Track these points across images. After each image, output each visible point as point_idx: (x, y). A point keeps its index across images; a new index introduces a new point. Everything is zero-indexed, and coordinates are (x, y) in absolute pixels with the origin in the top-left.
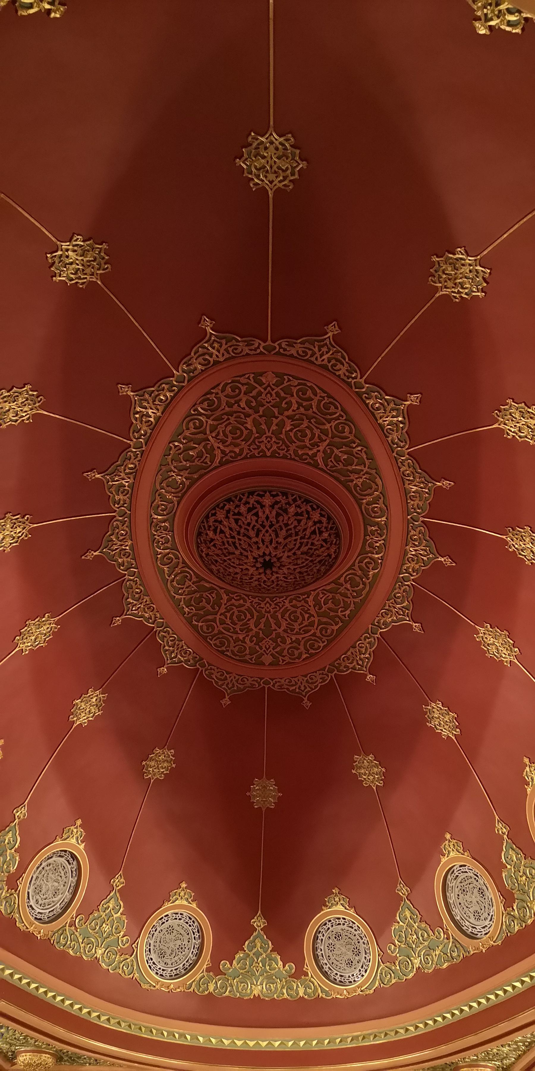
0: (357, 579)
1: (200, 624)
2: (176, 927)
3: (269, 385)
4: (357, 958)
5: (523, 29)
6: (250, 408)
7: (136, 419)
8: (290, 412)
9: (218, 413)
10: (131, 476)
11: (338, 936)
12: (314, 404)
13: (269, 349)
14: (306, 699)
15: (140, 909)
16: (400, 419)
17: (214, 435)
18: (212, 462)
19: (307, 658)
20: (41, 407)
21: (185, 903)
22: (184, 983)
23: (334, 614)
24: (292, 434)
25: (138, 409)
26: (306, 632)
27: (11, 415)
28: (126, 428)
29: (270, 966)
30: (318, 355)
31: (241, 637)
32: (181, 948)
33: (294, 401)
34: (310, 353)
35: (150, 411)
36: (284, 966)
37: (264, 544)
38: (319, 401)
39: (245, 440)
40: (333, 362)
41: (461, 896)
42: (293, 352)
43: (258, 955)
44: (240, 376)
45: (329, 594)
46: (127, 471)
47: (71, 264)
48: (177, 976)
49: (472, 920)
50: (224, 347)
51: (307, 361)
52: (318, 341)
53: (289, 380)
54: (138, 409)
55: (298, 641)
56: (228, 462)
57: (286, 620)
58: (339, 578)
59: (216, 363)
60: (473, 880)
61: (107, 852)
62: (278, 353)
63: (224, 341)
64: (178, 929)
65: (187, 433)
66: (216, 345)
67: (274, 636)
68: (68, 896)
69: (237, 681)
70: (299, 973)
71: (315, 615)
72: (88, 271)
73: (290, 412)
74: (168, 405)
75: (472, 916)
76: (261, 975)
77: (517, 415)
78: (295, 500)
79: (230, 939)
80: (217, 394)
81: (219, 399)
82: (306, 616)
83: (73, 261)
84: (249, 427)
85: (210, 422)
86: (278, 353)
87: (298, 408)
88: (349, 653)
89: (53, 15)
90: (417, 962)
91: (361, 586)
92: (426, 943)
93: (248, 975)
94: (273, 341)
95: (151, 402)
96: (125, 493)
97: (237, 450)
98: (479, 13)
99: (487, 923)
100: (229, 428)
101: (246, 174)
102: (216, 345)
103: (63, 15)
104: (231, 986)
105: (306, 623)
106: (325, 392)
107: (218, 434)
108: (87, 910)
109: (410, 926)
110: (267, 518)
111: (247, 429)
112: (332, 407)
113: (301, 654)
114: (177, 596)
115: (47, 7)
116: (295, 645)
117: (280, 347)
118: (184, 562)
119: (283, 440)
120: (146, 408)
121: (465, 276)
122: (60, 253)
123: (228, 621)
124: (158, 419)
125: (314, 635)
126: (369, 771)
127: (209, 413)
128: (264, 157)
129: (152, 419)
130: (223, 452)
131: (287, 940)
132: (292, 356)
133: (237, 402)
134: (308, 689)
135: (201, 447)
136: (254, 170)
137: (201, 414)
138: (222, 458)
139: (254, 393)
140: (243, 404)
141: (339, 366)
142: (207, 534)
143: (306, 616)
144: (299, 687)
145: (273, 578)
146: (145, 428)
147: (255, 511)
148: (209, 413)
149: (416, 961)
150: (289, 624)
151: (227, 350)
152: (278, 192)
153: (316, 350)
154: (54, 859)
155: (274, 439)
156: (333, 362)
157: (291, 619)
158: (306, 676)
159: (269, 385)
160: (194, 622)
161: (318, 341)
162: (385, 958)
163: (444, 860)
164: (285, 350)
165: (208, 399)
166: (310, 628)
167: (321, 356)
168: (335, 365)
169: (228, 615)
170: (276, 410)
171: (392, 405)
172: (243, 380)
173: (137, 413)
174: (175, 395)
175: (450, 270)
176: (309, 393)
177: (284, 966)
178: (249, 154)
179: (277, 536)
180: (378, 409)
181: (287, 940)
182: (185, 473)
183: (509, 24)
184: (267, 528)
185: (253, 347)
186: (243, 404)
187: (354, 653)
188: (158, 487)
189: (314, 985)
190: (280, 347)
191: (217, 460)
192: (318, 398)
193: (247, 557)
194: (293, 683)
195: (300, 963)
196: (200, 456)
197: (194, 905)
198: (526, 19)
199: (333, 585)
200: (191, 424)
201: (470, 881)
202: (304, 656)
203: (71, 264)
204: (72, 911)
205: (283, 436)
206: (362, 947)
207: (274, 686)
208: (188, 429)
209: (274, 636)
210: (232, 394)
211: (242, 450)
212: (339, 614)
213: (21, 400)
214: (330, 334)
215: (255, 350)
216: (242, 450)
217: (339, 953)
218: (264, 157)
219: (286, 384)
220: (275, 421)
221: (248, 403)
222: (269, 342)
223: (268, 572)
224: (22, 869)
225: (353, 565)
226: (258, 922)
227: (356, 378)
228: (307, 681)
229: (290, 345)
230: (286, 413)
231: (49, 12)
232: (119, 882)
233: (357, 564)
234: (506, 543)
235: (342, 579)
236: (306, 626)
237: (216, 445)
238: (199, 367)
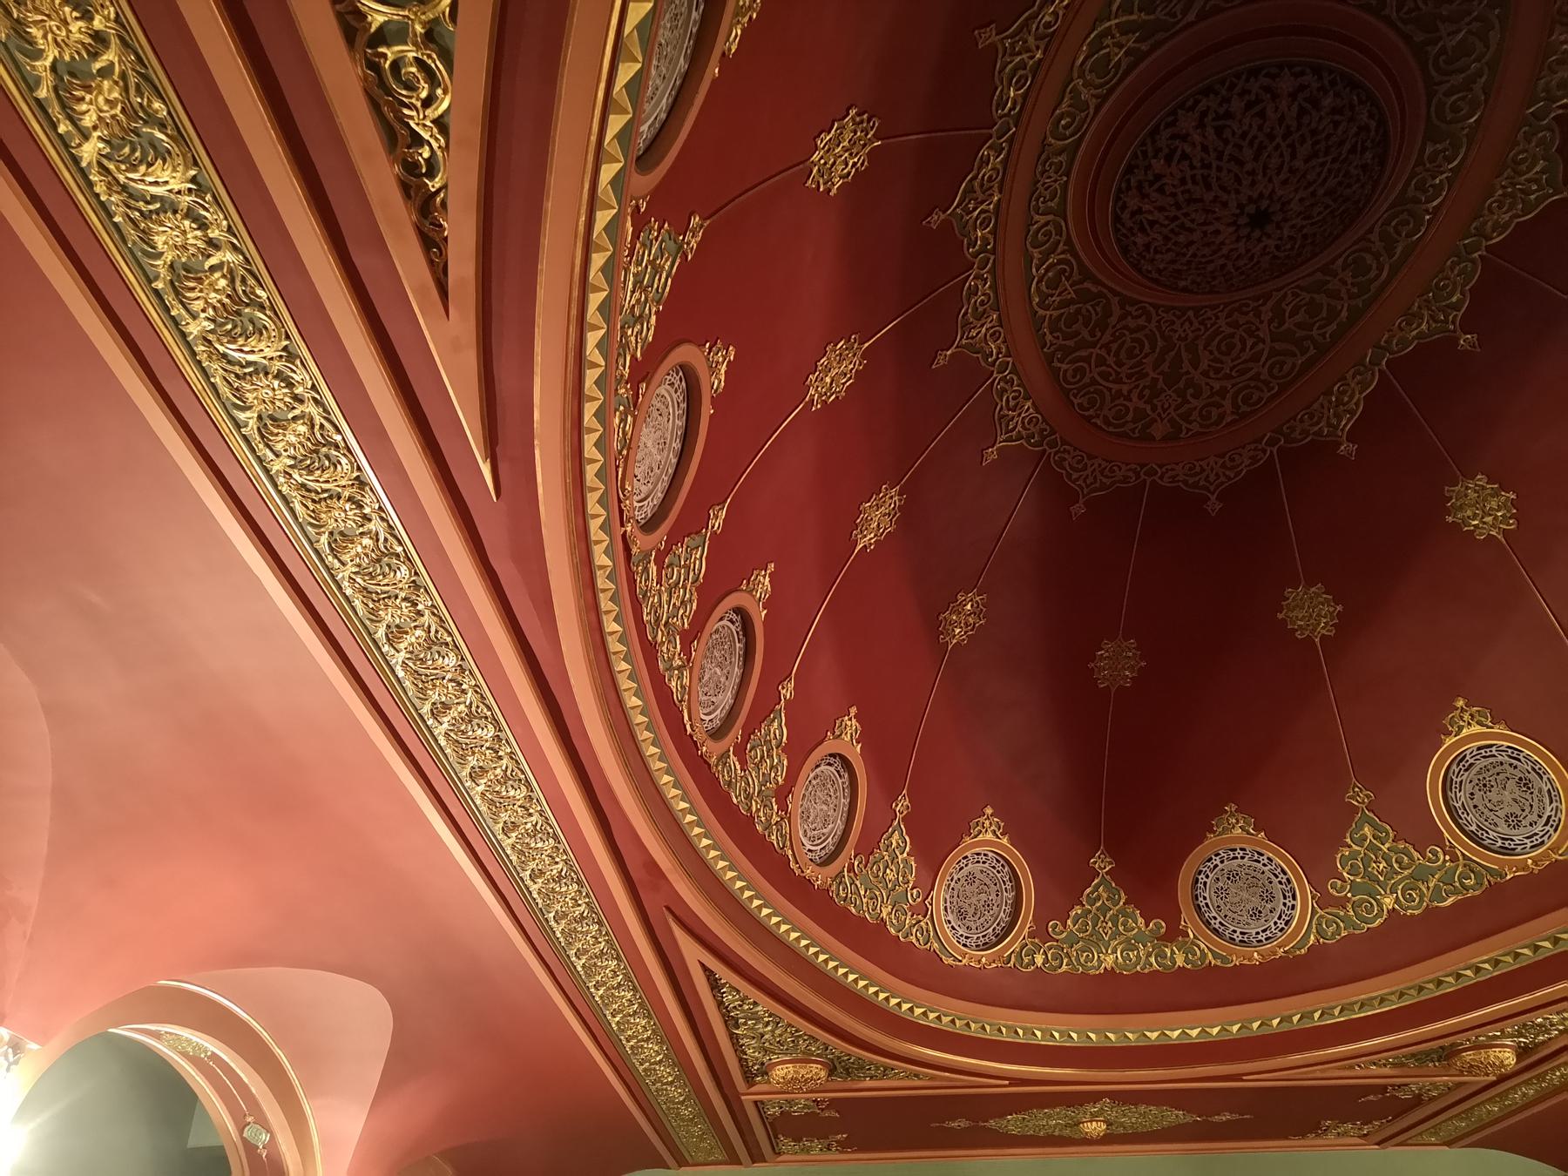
0: (1369, 258)
1: (1064, 366)
2: (978, 875)
4: (1269, 906)
11: (1232, 876)
14: (1213, 498)
15: (933, 849)
19: (1233, 422)
21: (989, 836)
22: (999, 955)
23: (1304, 333)
26: (1242, 373)
29: (1124, 924)
31: (1125, 389)
32: (987, 905)
36: (1147, 925)
37: (1229, 193)
41: (1478, 795)
43: (1104, 910)
45: (1304, 294)
48: (988, 946)
49: (1503, 828)
55: (1223, 393)
57: (1211, 352)
58: (1333, 261)
60: (1506, 766)
61: (887, 758)
64: (981, 876)
67: (1181, 385)
68: (840, 825)
69: (1102, 473)
70: (1174, 934)
71: (1268, 340)
75: (1501, 823)
76: (1113, 938)
78: (1333, 83)
79: (1063, 889)
82: (1249, 343)
88: (1316, 406)
90: (1388, 902)
91: (1373, 274)
92: (1406, 873)
93: (1095, 941)
99: (1538, 829)
104: (1068, 955)
105: (1245, 356)
108: (868, 847)
109: (1372, 848)
110: (1282, 119)
113: (1221, 417)
114: (1041, 312)
116: (1217, 398)
118: (1069, 242)
123: (1111, 360)
125: (1256, 377)
126: (1311, 613)
131: (1153, 886)
134: (1223, 479)
142: (1149, 167)
143: (1249, 343)
144: (1207, 479)
145: (1286, 232)
147: (1257, 109)
149: (1387, 900)
150: (1215, 360)
154: (822, 767)
157: (1221, 353)
158: (1222, 456)
160: (1056, 364)
162: (1324, 901)
163: (1449, 741)
166: (1250, 365)
169: (1114, 346)
177: (1147, 925)
179: (1293, 156)
181: (1153, 886)
184: (1279, 140)
187: (1326, 405)
189: (1199, 949)
193: (1225, 205)
194: (1198, 469)
195: (1172, 917)
197: (1005, 841)
199: (1319, 275)
201: (1498, 769)
202: (1229, 419)
204: (849, 850)
206: (1277, 889)
207: (1161, 478)
209: (1181, 385)
212: (1315, 332)
217: (1237, 899)
223: (1269, 228)
224: (792, 778)
225: (1371, 231)
226: (1102, 863)
228: (1223, 466)
232: (902, 805)
233: (1377, 229)
236: (1246, 361)
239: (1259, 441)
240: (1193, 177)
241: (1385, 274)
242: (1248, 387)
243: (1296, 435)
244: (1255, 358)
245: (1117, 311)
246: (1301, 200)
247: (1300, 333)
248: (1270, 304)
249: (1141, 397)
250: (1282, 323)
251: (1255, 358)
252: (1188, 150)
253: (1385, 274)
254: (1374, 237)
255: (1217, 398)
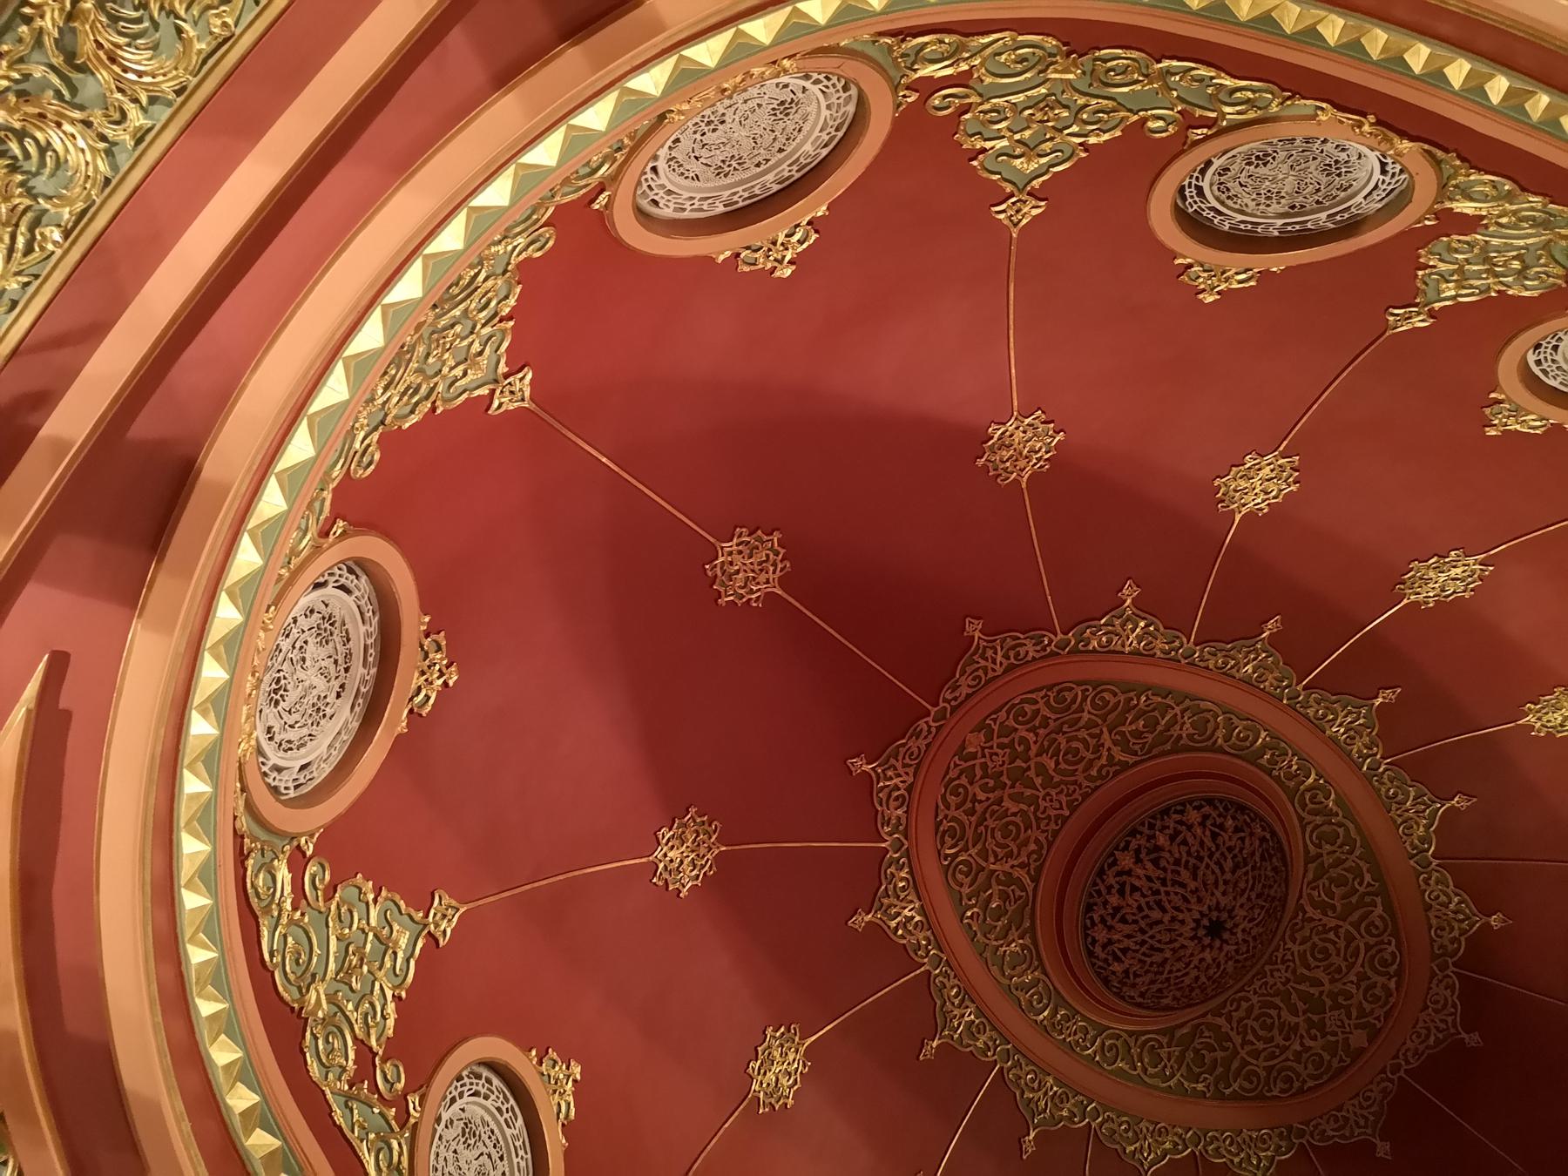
3: (983, 749)
5: (816, 232)
6: (993, 790)
7: (902, 937)
8: (1034, 749)
9: (970, 833)
10: (967, 1003)
12: (1046, 712)
13: (941, 716)
14: (1464, 1035)
16: (1142, 624)
17: (992, 860)
18: (1023, 889)
20: (803, 1038)
24: (1063, 766)
25: (893, 924)
27: (784, 1081)
28: (905, 958)
30: (990, 665)
33: (1024, 734)
34: (980, 673)
35: (906, 912)
38: (1047, 704)
39: (1028, 827)
40: (1012, 654)
42: (965, 691)
44: (947, 773)
46: (956, 1002)
47: (682, 862)
50: (899, 765)
51: (987, 682)
52: (974, 654)
53: (995, 720)
54: (893, 924)
55: (1362, 977)
56: (1039, 870)
58: (1307, 851)
59: (909, 790)
62: (954, 709)
63: (892, 761)
65: (966, 890)
66: (890, 773)
67: (1329, 1002)
69: (1362, 1107)
72: (702, 851)
73: (1034, 749)
74: (915, 884)
77: (1243, 484)
78: (1152, 827)
80: (946, 817)
81: (954, 819)
82: (1331, 935)
83: (681, 858)
84: (1014, 810)
85: (973, 851)
86: (954, 709)
87: (1037, 735)
88: (1434, 921)
89: (451, 683)
91: (1341, 831)
94: (936, 704)
95: (895, 902)
96: (981, 1029)
97: (1033, 847)
98: (769, 266)
100: (998, 834)
101: (739, 603)
102: (890, 773)
103: (459, 672)
105: (1342, 944)
106: (1040, 690)
107: (996, 856)
110: (1149, 879)
111: (1014, 814)
112: (1066, 694)
113: (1384, 986)
114: (1171, 1083)
115: (440, 682)
116: (1364, 985)
117: (949, 702)
118: (1131, 1034)
119: (1061, 782)
120: (899, 914)
121: (1026, 442)
122: (661, 866)
123: (1260, 1045)
124: (922, 911)
125: (1368, 948)
127: (961, 844)
128: (738, 572)
129: (918, 918)
130: (1022, 866)
132: (968, 696)
133: (974, 800)
135: (996, 888)
136: (742, 591)
137: (956, 855)
138: (1028, 873)
139: (979, 772)
140: (981, 796)
141: (1022, 651)
142: (1114, 973)
143: (1331, 935)
145: (1240, 935)
146: (921, 936)
147: (1128, 889)
148: (961, 844)
151: (904, 766)
152: (783, 582)
153: (983, 663)
155: (1053, 792)
156: (1012, 654)
157: (1320, 960)
159: (983, 749)
160: (1227, 1092)
161: (974, 654)
164: (955, 699)
165: (944, 832)
166: (1353, 945)
167: (994, 662)
168: (1018, 654)
169: (1250, 1037)
170: (1019, 763)
171: (1117, 622)
172: (951, 775)
173: (896, 929)
174: (910, 867)
175: (1006, 454)
176: (1027, 707)
178: (723, 584)
179: (1183, 885)
180: (1109, 642)
182: (1014, 934)
183: (801, 242)
184: (1162, 889)
185: (925, 733)
186: (981, 796)
188: (1006, 982)
190: (949, 702)
191: (1027, 881)
192: (1041, 702)
193: (1183, 947)
194: (1424, 1032)
196: (1005, 897)
198: (809, 223)
199: (1312, 866)
200: (959, 876)
202: (1392, 985)
203: (682, 862)
205: (1057, 779)
207: (1408, 1062)
208: (961, 885)
209: (1329, 1002)
210: (961, 798)
211: (1037, 841)
212: (1362, 889)
213: (777, 1054)
214: (977, 634)
215: (929, 732)
216: (1037, 841)
218: (738, 572)
219: (996, 728)
220: (1032, 774)
221: (984, 788)
222: (933, 710)
223: (1226, 936)
225: (1301, 819)
227: (1051, 641)
229: (955, 688)
230: (1032, 753)
231: (445, 684)
233: (1304, 815)
234: (1417, 604)
235: (1311, 847)
236: (1347, 947)
237: (1007, 868)
238: (899, 812)
239: (1434, 975)
240: (1144, 954)
241: (1351, 827)
242: (1373, 957)
243: (1450, 948)
244: (1350, 939)
245: (1221, 1021)
246: (1224, 893)
247: (1354, 900)
248: (1308, 908)
249: (1314, 1038)
250: (1333, 908)
251: (1350, 939)
252: (1137, 883)
253: (1351, 827)
254: (1308, 818)
255: (1364, 985)
